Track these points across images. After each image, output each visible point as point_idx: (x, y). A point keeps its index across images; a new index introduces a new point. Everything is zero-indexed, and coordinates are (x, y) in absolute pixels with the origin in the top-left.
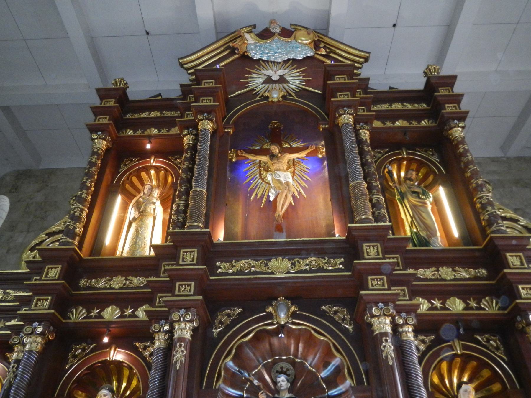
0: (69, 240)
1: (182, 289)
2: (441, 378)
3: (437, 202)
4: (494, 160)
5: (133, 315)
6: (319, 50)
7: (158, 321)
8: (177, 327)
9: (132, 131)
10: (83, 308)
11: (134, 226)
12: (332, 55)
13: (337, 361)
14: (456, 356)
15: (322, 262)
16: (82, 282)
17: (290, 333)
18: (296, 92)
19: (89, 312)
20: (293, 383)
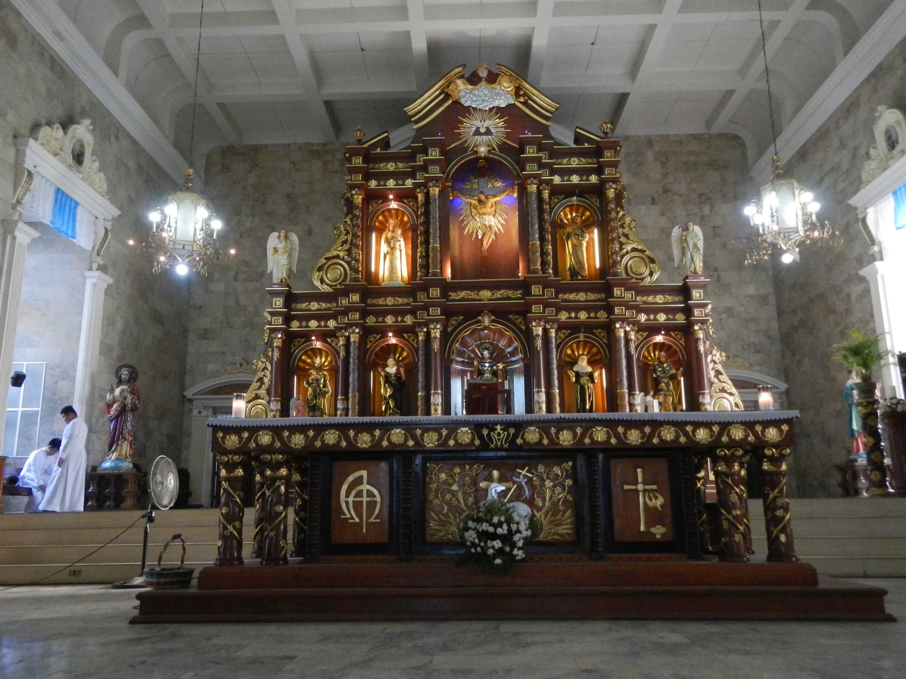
0: (357, 276)
1: (433, 311)
2: (573, 351)
3: (592, 240)
4: (696, 137)
5: (403, 321)
6: (519, 98)
7: (420, 326)
8: (432, 331)
9: (373, 181)
10: (373, 316)
11: (388, 256)
12: (529, 102)
13: (516, 344)
14: (580, 341)
15: (510, 293)
16: (369, 301)
17: (490, 329)
18: (498, 146)
19: (377, 319)
20: (491, 354)
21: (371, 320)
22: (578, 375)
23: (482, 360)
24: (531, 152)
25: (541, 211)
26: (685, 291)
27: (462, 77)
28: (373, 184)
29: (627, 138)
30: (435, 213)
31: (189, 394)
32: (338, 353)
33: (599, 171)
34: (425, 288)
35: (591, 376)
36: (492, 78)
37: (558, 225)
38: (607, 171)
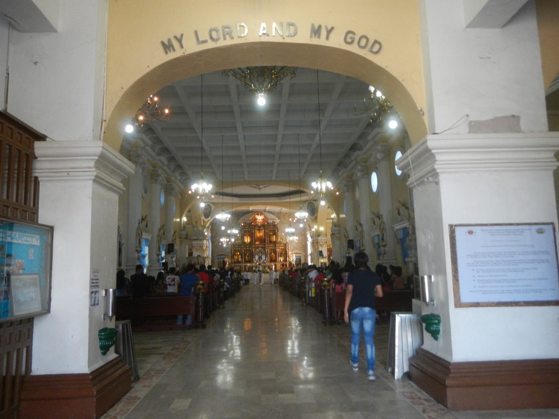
21: (245, 249)
22: (272, 255)
23: (259, 253)
24: (266, 226)
25: (267, 234)
26: (286, 244)
27: (256, 214)
28: (245, 230)
29: (282, 213)
30: (253, 235)
31: (214, 256)
32: (240, 252)
33: (275, 228)
34: (252, 245)
35: (273, 255)
36: (261, 215)
37: (270, 235)
38: (276, 228)
